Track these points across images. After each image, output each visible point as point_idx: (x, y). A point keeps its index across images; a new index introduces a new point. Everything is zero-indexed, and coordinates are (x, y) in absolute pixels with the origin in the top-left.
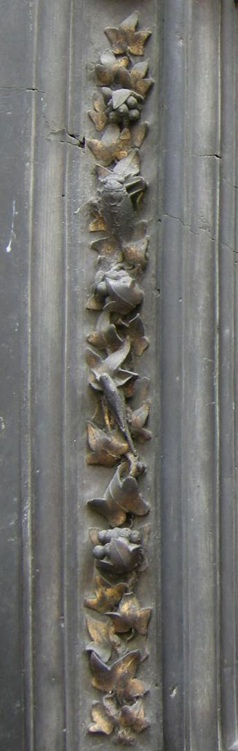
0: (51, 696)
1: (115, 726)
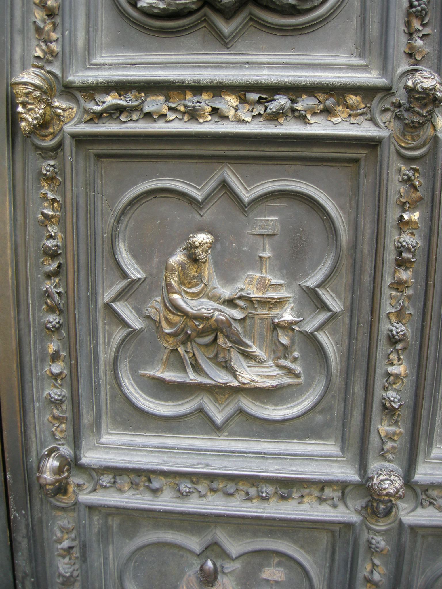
0: (18, 39)
1: (45, 53)
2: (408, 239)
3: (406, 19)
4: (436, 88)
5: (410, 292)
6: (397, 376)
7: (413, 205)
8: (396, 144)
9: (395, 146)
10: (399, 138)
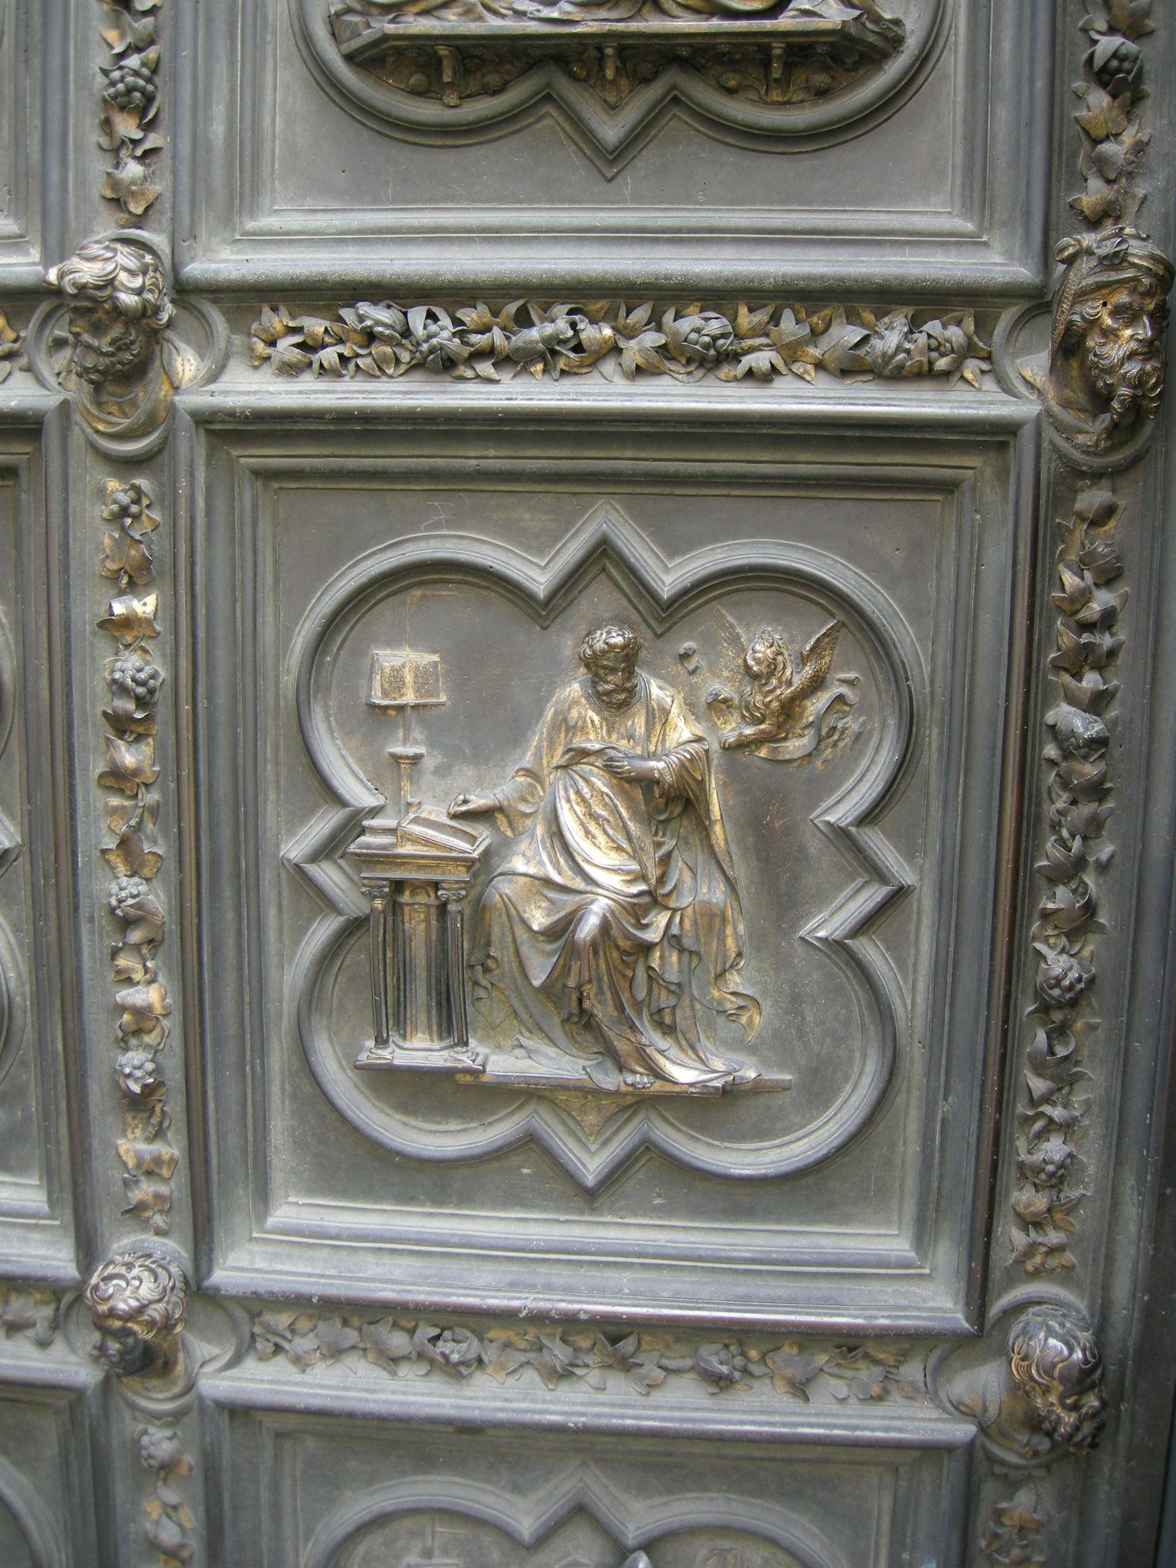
2: (130, 664)
3: (102, 117)
4: (116, 283)
5: (152, 797)
6: (142, 1013)
7: (134, 582)
8: (85, 425)
9: (83, 431)
10: (89, 412)
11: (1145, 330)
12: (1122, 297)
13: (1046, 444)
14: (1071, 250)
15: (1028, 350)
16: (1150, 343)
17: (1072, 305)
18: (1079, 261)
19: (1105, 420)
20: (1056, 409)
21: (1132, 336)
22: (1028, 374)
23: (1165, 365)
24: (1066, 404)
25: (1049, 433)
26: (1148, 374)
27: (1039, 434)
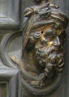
11: (57, 42)
12: (49, 30)
13: (20, 85)
14: (30, 12)
15: (13, 49)
16: (59, 47)
17: (30, 33)
18: (32, 16)
19: (42, 75)
20: (24, 71)
21: (52, 44)
22: (13, 58)
23: (65, 55)
24: (28, 70)
25: (21, 80)
26: (59, 58)
27: (17, 81)
